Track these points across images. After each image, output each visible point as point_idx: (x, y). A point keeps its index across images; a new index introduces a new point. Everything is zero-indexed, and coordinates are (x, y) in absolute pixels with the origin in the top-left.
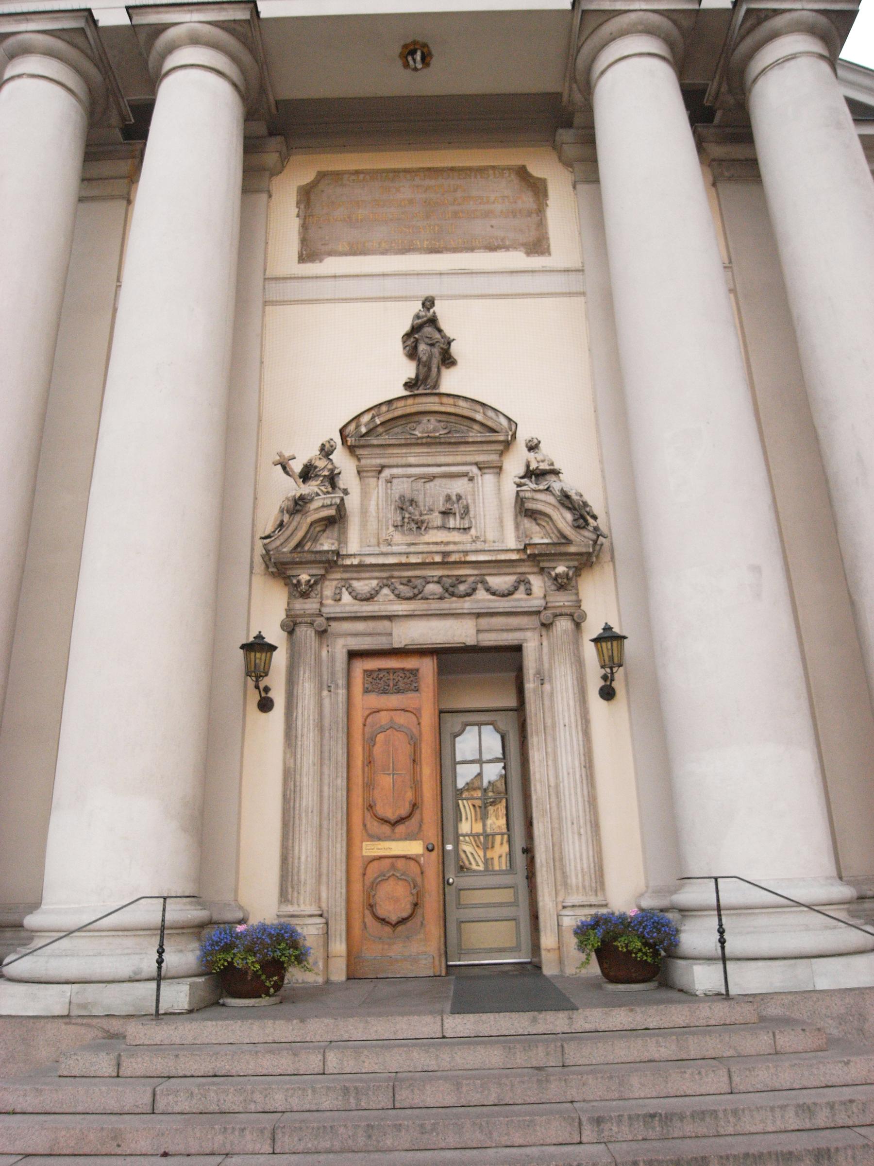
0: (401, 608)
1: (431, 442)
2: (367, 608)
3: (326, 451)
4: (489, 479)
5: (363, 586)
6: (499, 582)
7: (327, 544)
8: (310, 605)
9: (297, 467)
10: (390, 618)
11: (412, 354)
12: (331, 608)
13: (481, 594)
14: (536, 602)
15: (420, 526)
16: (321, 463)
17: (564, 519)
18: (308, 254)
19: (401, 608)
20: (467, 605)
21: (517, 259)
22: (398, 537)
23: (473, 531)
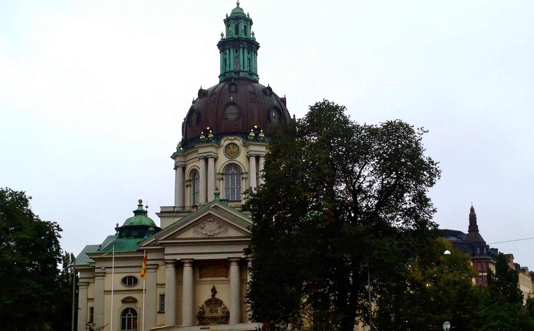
0: (210, 322)
1: (213, 304)
2: (207, 322)
3: (203, 306)
4: (219, 308)
5: (207, 319)
6: (220, 319)
7: (203, 316)
8: (201, 322)
9: (200, 307)
10: (210, 323)
11: (212, 292)
12: (204, 322)
13: (218, 320)
14: (223, 321)
15: (213, 313)
16: (202, 307)
17: (226, 314)
18: (201, 277)
19: (210, 322)
20: (217, 321)
21: (224, 278)
22: (210, 314)
23: (218, 313)
